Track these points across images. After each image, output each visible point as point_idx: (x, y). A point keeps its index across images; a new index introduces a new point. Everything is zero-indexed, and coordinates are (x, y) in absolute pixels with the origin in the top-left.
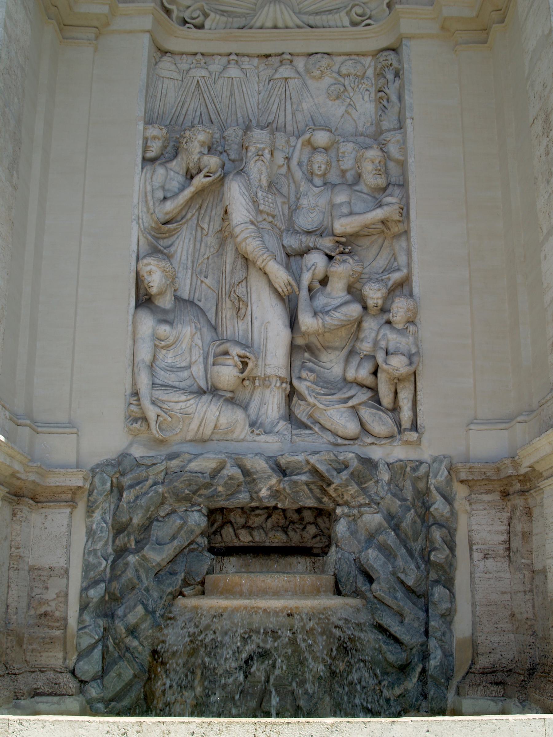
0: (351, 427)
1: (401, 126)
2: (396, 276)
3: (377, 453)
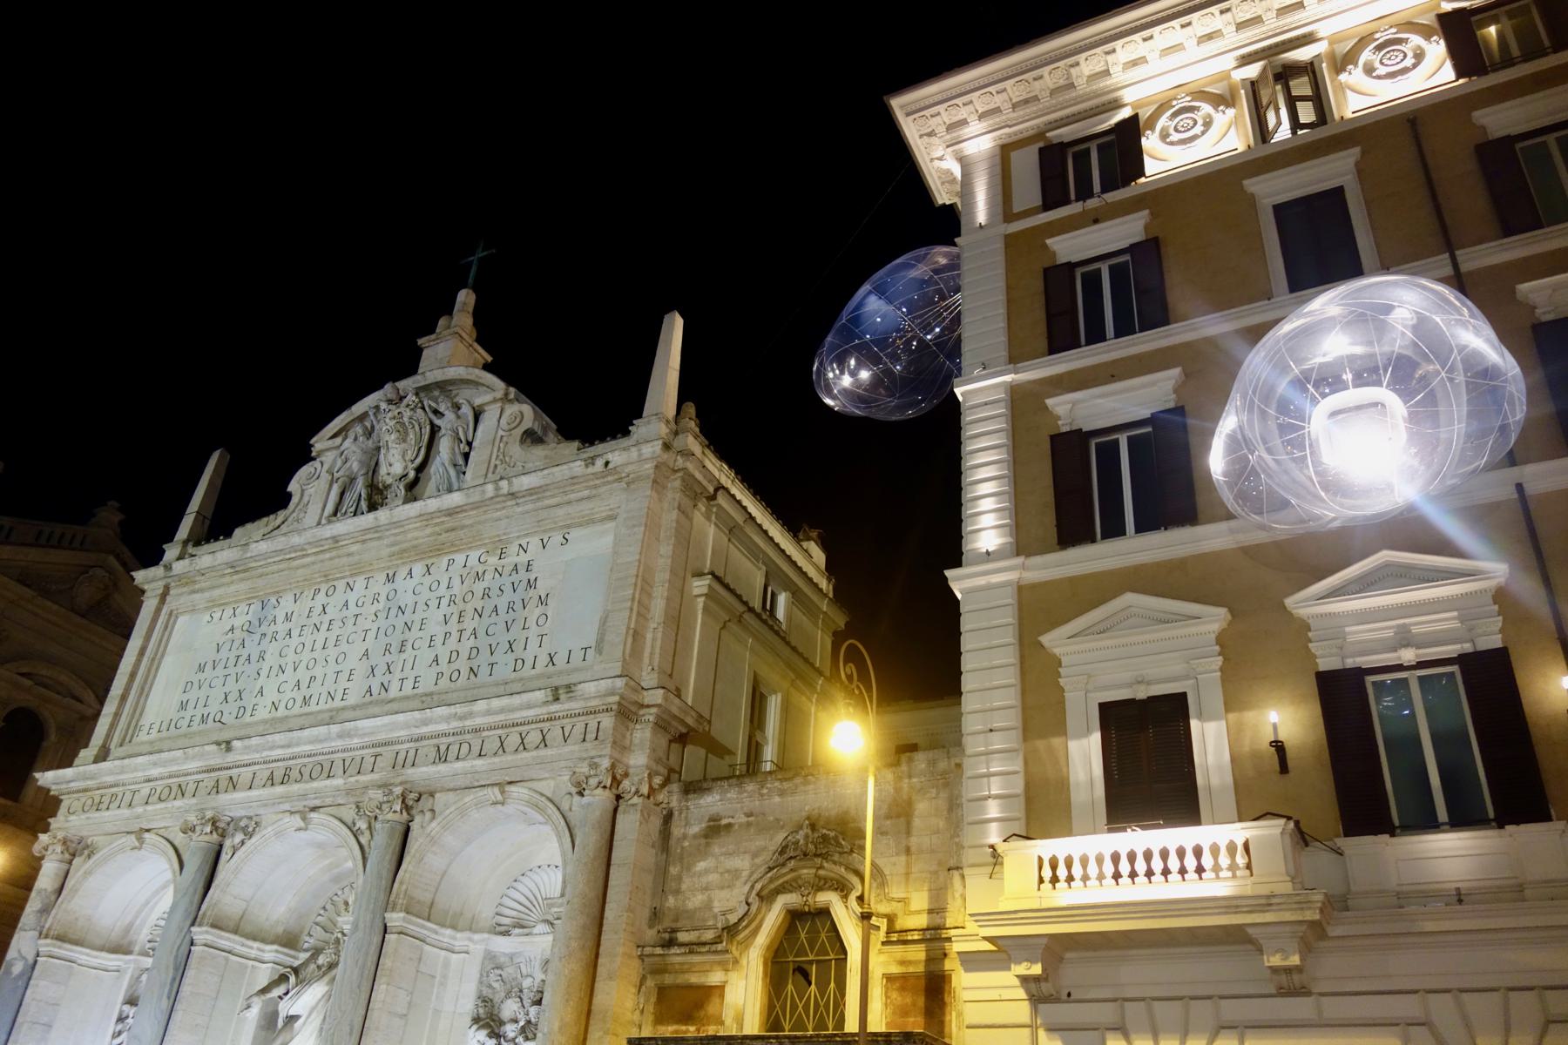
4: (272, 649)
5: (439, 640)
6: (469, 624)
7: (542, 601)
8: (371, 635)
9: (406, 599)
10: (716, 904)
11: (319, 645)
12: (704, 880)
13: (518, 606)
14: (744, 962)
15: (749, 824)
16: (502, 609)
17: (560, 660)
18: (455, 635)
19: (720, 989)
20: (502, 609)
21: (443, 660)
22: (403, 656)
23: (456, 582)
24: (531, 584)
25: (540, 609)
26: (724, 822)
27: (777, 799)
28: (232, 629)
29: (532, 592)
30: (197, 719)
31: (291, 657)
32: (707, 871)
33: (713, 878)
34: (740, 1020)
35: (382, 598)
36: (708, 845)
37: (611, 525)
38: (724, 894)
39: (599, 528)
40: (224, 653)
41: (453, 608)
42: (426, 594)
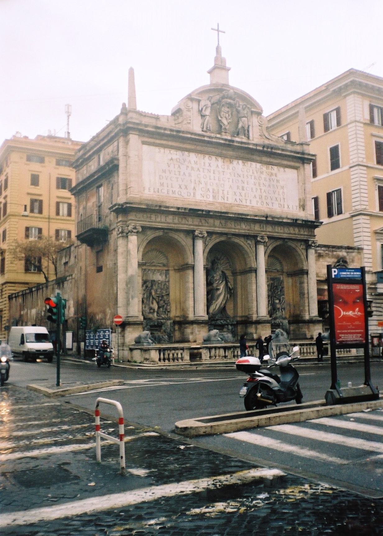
7: (282, 187)
8: (231, 180)
11: (212, 178)
13: (276, 187)
23: (255, 172)
25: (281, 191)
28: (172, 159)
30: (171, 192)
37: (295, 171)
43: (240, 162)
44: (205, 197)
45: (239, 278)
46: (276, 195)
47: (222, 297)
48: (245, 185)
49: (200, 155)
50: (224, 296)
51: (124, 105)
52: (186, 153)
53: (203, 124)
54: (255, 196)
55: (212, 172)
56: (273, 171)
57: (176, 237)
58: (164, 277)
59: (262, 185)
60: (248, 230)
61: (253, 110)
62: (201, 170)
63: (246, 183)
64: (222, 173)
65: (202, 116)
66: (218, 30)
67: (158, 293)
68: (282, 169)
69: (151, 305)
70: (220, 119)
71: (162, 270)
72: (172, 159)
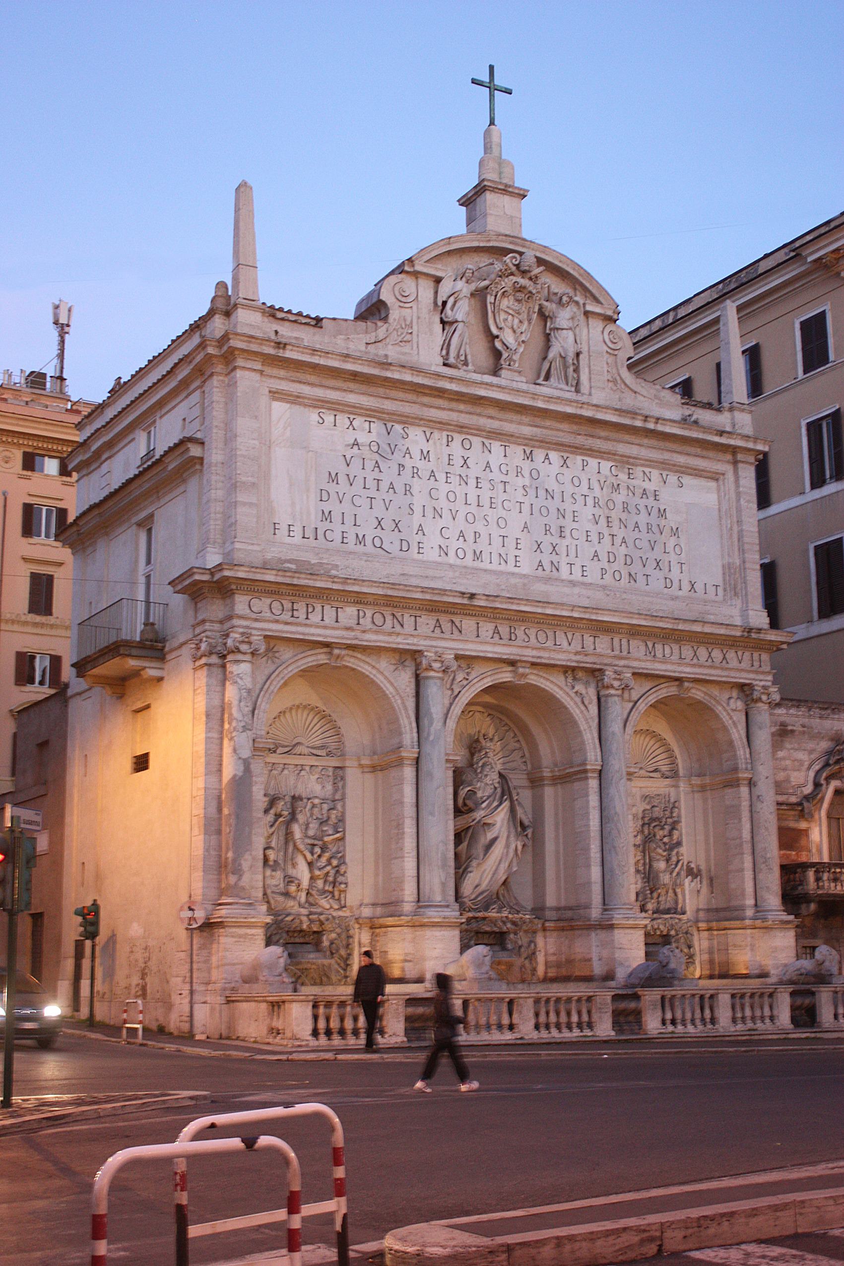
0: (328, 907)
1: (343, 799)
2: (340, 855)
3: (335, 914)
4: (417, 485)
5: (594, 537)
6: (620, 533)
7: (675, 532)
8: (526, 508)
9: (552, 485)
10: (792, 779)
11: (472, 499)
12: (783, 763)
14: (816, 816)
15: (804, 733)
16: (643, 527)
17: (699, 587)
18: (607, 540)
19: (806, 832)
20: (643, 527)
21: (603, 556)
22: (565, 542)
24: (662, 513)
25: (672, 542)
26: (790, 728)
27: (818, 720)
28: (356, 444)
29: (663, 522)
30: (351, 539)
31: (443, 503)
32: (784, 759)
33: (788, 762)
34: (820, 851)
35: (526, 473)
36: (782, 741)
37: (713, 484)
38: (796, 774)
39: (702, 482)
40: (355, 468)
41: (597, 511)
42: (569, 489)
43: (554, 456)
44: (451, 553)
45: (549, 792)
46: (658, 553)
47: (498, 850)
48: (568, 523)
49: (436, 435)
50: (507, 846)
51: (221, 285)
52: (398, 427)
53: (447, 345)
54: (596, 555)
55: (472, 482)
56: (646, 485)
57: (366, 669)
58: (329, 787)
59: (616, 523)
60: (577, 653)
61: (589, 308)
62: (441, 477)
63: (569, 516)
64: (501, 486)
65: (442, 322)
66: (492, 87)
67: (311, 833)
68: (672, 478)
69: (291, 872)
70: (495, 331)
71: (325, 768)
72: (356, 444)
